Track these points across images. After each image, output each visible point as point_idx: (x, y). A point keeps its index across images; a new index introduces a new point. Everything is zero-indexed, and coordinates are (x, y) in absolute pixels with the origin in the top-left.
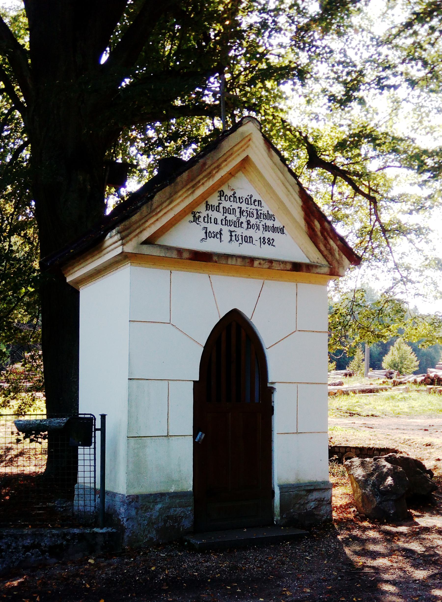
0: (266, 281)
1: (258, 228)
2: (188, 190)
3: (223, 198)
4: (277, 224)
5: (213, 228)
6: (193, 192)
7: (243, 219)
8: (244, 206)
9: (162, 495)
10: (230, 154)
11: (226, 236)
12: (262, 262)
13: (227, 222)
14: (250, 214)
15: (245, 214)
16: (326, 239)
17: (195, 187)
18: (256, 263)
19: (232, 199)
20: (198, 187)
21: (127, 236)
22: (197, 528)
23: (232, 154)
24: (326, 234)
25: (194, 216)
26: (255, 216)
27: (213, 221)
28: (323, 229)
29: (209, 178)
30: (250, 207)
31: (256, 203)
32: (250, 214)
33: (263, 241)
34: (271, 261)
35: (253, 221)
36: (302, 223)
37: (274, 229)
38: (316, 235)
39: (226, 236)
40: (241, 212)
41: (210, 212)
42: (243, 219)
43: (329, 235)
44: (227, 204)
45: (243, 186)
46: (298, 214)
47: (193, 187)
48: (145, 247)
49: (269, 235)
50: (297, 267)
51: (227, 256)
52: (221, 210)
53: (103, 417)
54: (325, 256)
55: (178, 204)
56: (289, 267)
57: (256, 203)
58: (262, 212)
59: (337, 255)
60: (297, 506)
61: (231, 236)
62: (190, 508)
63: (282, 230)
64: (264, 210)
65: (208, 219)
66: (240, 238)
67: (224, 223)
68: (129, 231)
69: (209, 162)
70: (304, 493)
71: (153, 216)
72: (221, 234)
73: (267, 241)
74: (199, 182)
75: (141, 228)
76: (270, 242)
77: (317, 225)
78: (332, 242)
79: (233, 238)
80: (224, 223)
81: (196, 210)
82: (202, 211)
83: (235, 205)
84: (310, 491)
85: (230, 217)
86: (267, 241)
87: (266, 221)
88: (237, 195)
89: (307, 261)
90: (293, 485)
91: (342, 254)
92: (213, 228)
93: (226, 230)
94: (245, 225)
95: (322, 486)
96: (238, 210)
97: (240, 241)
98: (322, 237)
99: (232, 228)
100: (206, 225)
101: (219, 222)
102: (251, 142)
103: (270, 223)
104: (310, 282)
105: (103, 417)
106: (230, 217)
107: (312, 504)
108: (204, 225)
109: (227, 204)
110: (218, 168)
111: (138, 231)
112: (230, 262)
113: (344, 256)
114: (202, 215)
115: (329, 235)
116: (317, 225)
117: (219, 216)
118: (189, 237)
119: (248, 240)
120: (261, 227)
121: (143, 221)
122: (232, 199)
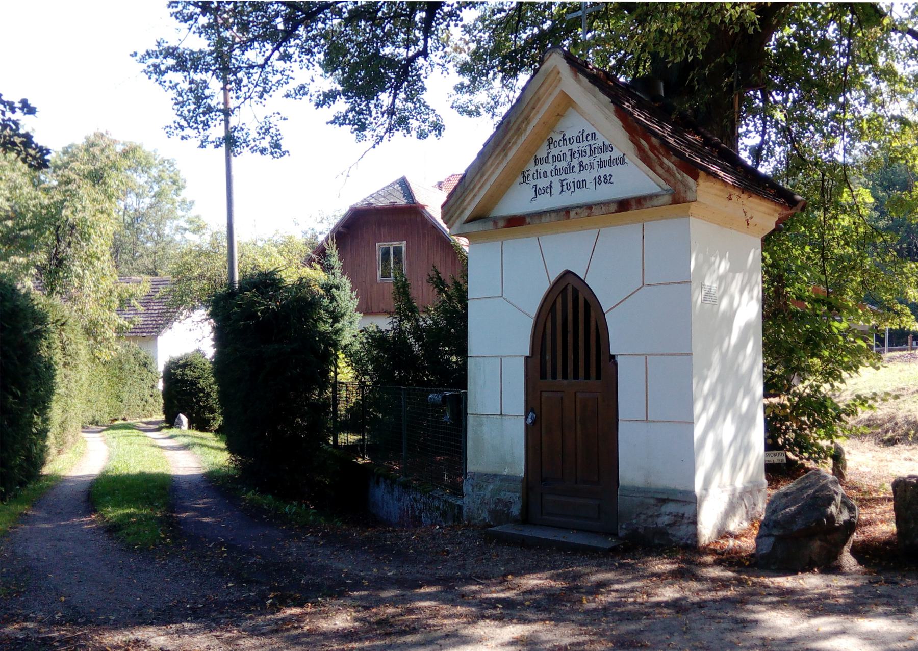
2: (498, 155)
3: (552, 146)
4: (616, 154)
5: (542, 183)
6: (506, 155)
8: (575, 147)
9: (495, 475)
12: (579, 210)
13: (557, 171)
14: (582, 153)
15: (577, 155)
17: (506, 149)
18: (572, 214)
19: (561, 143)
20: (510, 148)
22: (526, 518)
26: (588, 154)
30: (581, 144)
31: (589, 138)
32: (582, 153)
33: (598, 181)
35: (586, 160)
37: (611, 162)
38: (649, 157)
40: (572, 155)
41: (539, 167)
44: (555, 151)
47: (503, 149)
48: (466, 225)
49: (604, 171)
50: (623, 205)
51: (540, 214)
55: (493, 172)
56: (613, 207)
57: (589, 138)
58: (596, 146)
60: (643, 517)
61: (562, 185)
62: (518, 495)
63: (622, 161)
65: (537, 176)
66: (572, 185)
68: (449, 214)
70: (652, 501)
71: (469, 194)
73: (602, 179)
76: (607, 179)
78: (666, 161)
79: (565, 188)
82: (532, 168)
83: (565, 149)
84: (664, 501)
86: (602, 179)
87: (600, 156)
88: (567, 137)
89: (659, 189)
90: (638, 488)
92: (542, 183)
93: (556, 181)
94: (577, 169)
95: (680, 497)
96: (568, 154)
99: (563, 177)
100: (535, 182)
101: (549, 174)
103: (605, 156)
104: (662, 218)
107: (666, 520)
108: (533, 182)
109: (555, 151)
112: (543, 219)
113: (685, 175)
117: (548, 167)
120: (596, 166)
122: (561, 143)
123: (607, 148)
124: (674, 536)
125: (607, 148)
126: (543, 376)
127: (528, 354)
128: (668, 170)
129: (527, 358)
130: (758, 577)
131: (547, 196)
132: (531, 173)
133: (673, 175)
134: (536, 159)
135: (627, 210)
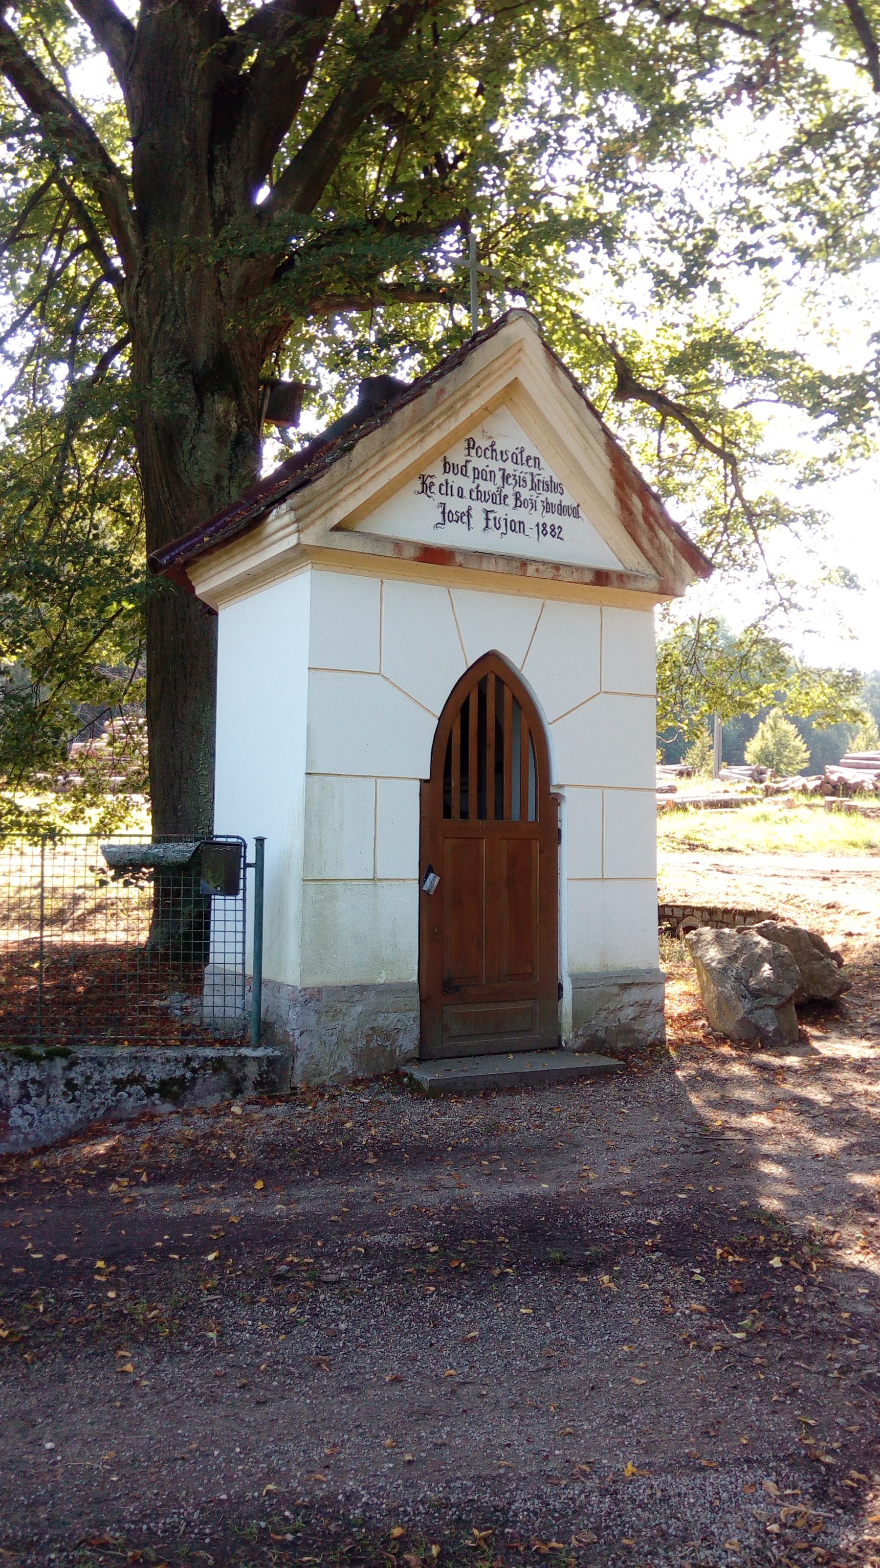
0: (548, 602)
1: (534, 507)
2: (413, 436)
3: (473, 452)
4: (568, 500)
5: (456, 504)
6: (422, 441)
7: (508, 490)
8: (510, 467)
9: (363, 988)
10: (486, 374)
11: (478, 519)
12: (541, 568)
13: (480, 495)
15: (511, 480)
16: (651, 528)
17: (425, 431)
18: (531, 569)
19: (489, 454)
21: (307, 515)
23: (489, 375)
24: (651, 519)
25: (424, 483)
27: (455, 492)
28: (647, 510)
29: (449, 417)
30: (519, 468)
31: (531, 462)
33: (543, 529)
34: (557, 567)
35: (525, 494)
36: (611, 499)
37: (562, 510)
39: (478, 519)
40: (505, 478)
41: (450, 477)
42: (508, 490)
43: (657, 522)
45: (509, 433)
46: (604, 483)
47: (422, 430)
48: (337, 535)
49: (552, 519)
50: (601, 578)
51: (481, 555)
52: (470, 473)
53: (260, 841)
54: (650, 560)
55: (396, 461)
56: (589, 577)
57: (531, 462)
59: (672, 559)
60: (603, 1014)
61: (487, 519)
62: (412, 1014)
63: (574, 512)
64: (545, 476)
65: (447, 489)
66: (503, 523)
67: (474, 496)
68: (310, 506)
69: (450, 388)
70: (615, 990)
72: (469, 516)
74: (432, 422)
75: (332, 503)
76: (555, 532)
77: (637, 504)
78: (662, 535)
80: (474, 496)
81: (426, 473)
83: (495, 465)
84: (626, 987)
85: (486, 486)
89: (619, 568)
90: (595, 974)
91: (680, 556)
93: (478, 508)
94: (511, 501)
95: (648, 978)
96: (499, 475)
97: (503, 529)
98: (644, 526)
99: (489, 506)
101: (466, 494)
102: (521, 355)
104: (624, 606)
105: (260, 841)
106: (486, 486)
107: (630, 1012)
108: (439, 498)
110: (466, 398)
111: (325, 507)
112: (485, 565)
113: (683, 561)
114: (437, 482)
115: (657, 522)
116: (637, 504)
117: (467, 483)
118: (415, 520)
119: (517, 527)
120: (539, 507)
121: (335, 489)
122: (489, 454)
123: (553, 486)
124: (640, 1032)
125: (553, 486)
126: (447, 813)
127: (427, 776)
128: (661, 551)
129: (423, 782)
130: (781, 1055)
131: (461, 527)
132: (437, 482)
133: (662, 555)
134: (446, 463)
135: (606, 585)
